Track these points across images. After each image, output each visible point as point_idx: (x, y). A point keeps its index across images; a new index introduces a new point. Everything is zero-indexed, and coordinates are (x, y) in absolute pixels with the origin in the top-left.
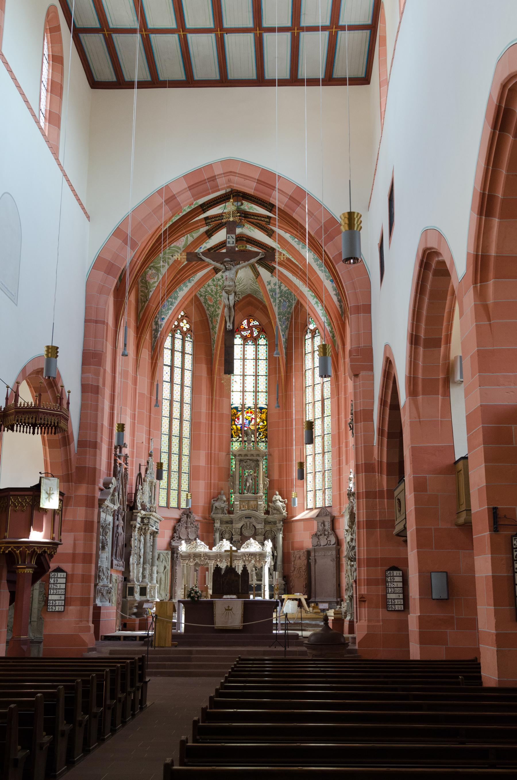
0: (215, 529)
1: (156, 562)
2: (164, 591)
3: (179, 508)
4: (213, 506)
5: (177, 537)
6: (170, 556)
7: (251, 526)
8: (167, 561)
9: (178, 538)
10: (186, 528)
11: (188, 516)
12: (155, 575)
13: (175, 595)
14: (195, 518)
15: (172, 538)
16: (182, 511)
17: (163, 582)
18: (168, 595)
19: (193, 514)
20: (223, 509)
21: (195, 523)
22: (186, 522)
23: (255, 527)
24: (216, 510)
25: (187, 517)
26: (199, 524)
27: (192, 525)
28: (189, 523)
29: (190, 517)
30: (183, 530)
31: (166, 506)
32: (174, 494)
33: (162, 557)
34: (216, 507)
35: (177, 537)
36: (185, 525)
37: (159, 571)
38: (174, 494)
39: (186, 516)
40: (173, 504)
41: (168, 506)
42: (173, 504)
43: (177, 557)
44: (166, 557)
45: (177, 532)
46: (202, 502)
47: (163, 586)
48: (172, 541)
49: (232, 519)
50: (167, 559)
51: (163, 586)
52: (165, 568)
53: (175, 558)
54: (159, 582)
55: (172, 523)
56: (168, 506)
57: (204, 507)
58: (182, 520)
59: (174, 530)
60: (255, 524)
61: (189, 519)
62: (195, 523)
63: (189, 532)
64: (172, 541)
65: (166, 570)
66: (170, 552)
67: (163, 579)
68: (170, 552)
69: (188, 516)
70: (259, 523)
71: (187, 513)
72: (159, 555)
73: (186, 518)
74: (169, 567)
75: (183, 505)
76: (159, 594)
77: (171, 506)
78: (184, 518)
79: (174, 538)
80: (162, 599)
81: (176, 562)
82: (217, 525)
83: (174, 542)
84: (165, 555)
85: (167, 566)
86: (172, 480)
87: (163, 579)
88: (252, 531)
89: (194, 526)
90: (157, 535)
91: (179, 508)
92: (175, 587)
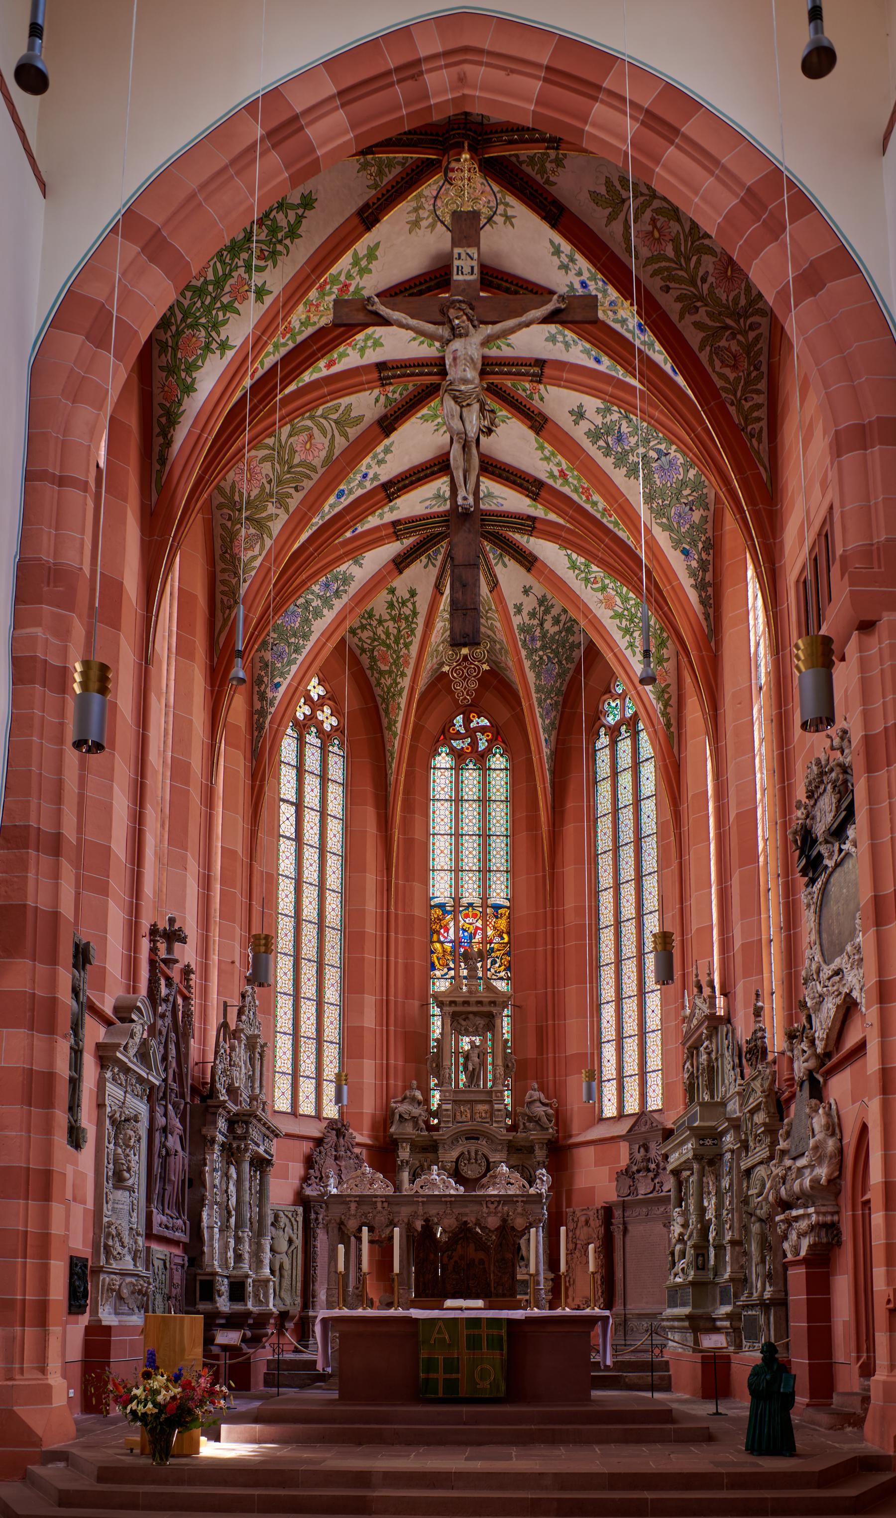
0: (399, 1163)
1: (270, 1231)
2: (289, 1293)
3: (318, 1116)
4: (393, 1113)
5: (316, 1178)
6: (300, 1219)
7: (479, 1157)
8: (295, 1227)
9: (317, 1180)
10: (336, 1158)
11: (340, 1133)
12: (267, 1256)
13: (313, 1302)
14: (355, 1138)
15: (305, 1179)
16: (325, 1124)
17: (287, 1274)
18: (299, 1300)
19: (351, 1131)
20: (415, 1120)
21: (357, 1150)
22: (336, 1145)
23: (487, 1160)
24: (401, 1122)
25: (338, 1136)
26: (364, 1151)
27: (349, 1153)
28: (343, 1149)
29: (344, 1136)
30: (330, 1161)
31: (289, 1110)
32: (307, 1087)
33: (283, 1220)
34: (400, 1116)
35: (316, 1178)
36: (334, 1153)
37: (276, 1248)
38: (307, 1087)
39: (334, 1132)
40: (307, 1107)
41: (294, 1112)
42: (307, 1107)
43: (317, 1219)
44: (293, 1219)
45: (316, 1166)
46: (369, 1106)
47: (286, 1282)
48: (304, 1186)
49: (435, 1141)
50: (294, 1223)
51: (286, 1282)
52: (290, 1241)
53: (313, 1222)
54: (277, 1273)
55: (306, 1147)
56: (294, 1112)
57: (374, 1116)
58: (325, 1140)
59: (309, 1162)
60: (486, 1151)
61: (341, 1140)
62: (357, 1150)
63: (342, 1168)
64: (304, 1186)
65: (292, 1248)
66: (301, 1208)
67: (287, 1266)
68: (300, 1210)
69: (340, 1133)
70: (496, 1150)
71: (338, 1128)
72: (276, 1217)
73: (335, 1138)
74: (298, 1242)
75: (331, 1111)
76: (277, 1298)
77: (301, 1112)
78: (332, 1137)
79: (309, 1179)
80: (283, 1308)
81: (314, 1232)
82: (404, 1153)
83: (310, 1188)
84: (290, 1216)
85: (294, 1237)
86: (303, 1056)
87: (287, 1266)
88: (480, 1165)
89: (352, 1157)
90: (272, 1171)
91: (318, 1116)
92: (313, 1285)
